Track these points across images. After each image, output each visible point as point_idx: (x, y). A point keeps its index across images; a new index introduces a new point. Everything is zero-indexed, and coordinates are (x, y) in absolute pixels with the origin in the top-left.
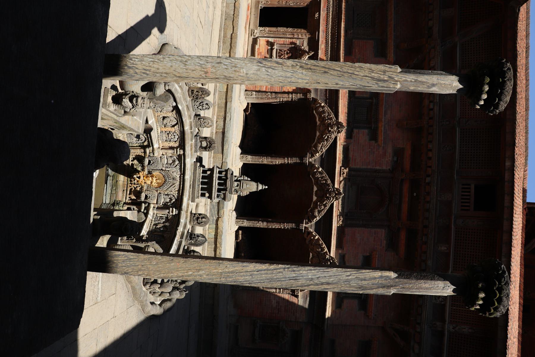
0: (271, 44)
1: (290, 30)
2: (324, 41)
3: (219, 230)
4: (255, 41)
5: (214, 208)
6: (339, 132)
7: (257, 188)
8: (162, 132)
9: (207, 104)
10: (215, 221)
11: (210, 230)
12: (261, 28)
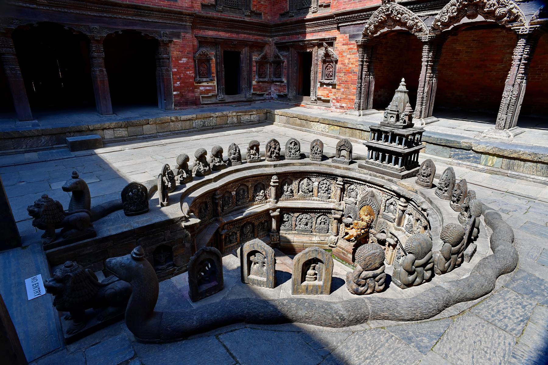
0: (322, 84)
1: (312, 68)
2: (320, 33)
3: (491, 152)
4: (319, 99)
5: (458, 155)
7: (401, 92)
8: (317, 196)
9: (291, 143)
10: (477, 155)
11: (490, 163)
12: (311, 94)
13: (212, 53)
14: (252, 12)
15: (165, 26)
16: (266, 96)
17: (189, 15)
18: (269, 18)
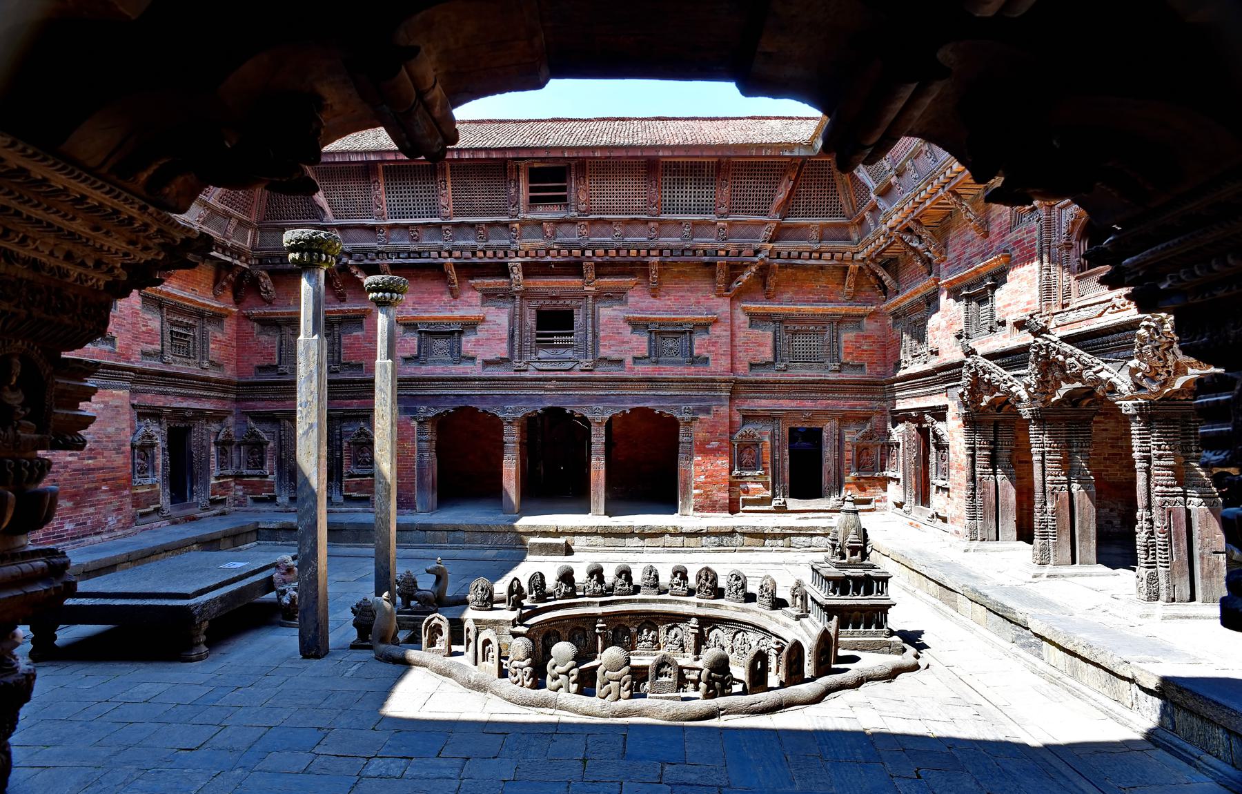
0: (938, 488)
6: (973, 352)
13: (763, 432)
14: (842, 365)
15: (688, 399)
16: (871, 506)
17: (726, 382)
18: (879, 369)
